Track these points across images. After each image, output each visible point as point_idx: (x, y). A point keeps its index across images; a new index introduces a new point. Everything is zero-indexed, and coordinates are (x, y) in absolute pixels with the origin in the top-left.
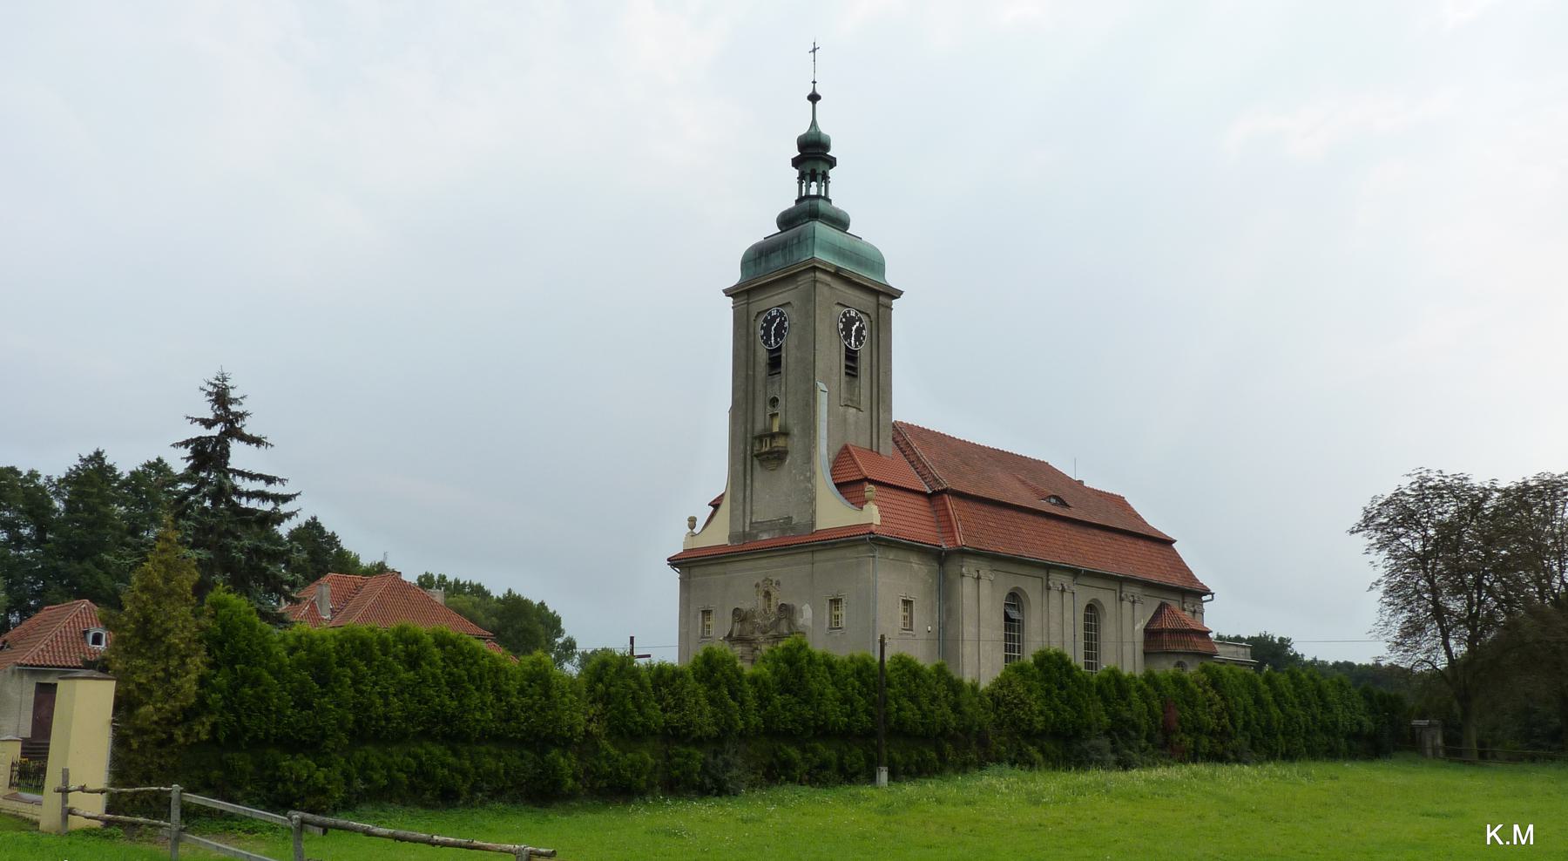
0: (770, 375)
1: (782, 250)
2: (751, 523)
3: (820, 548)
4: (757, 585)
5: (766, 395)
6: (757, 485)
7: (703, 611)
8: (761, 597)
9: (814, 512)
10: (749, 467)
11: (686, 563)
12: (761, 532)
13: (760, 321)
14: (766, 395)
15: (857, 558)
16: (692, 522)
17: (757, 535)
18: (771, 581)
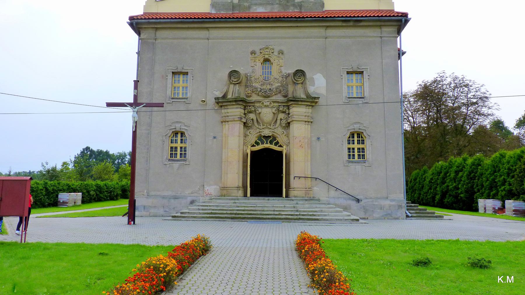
3: (340, 24)
4: (253, 53)
7: (173, 73)
8: (259, 64)
11: (155, 23)
12: (256, 4)
17: (249, 7)
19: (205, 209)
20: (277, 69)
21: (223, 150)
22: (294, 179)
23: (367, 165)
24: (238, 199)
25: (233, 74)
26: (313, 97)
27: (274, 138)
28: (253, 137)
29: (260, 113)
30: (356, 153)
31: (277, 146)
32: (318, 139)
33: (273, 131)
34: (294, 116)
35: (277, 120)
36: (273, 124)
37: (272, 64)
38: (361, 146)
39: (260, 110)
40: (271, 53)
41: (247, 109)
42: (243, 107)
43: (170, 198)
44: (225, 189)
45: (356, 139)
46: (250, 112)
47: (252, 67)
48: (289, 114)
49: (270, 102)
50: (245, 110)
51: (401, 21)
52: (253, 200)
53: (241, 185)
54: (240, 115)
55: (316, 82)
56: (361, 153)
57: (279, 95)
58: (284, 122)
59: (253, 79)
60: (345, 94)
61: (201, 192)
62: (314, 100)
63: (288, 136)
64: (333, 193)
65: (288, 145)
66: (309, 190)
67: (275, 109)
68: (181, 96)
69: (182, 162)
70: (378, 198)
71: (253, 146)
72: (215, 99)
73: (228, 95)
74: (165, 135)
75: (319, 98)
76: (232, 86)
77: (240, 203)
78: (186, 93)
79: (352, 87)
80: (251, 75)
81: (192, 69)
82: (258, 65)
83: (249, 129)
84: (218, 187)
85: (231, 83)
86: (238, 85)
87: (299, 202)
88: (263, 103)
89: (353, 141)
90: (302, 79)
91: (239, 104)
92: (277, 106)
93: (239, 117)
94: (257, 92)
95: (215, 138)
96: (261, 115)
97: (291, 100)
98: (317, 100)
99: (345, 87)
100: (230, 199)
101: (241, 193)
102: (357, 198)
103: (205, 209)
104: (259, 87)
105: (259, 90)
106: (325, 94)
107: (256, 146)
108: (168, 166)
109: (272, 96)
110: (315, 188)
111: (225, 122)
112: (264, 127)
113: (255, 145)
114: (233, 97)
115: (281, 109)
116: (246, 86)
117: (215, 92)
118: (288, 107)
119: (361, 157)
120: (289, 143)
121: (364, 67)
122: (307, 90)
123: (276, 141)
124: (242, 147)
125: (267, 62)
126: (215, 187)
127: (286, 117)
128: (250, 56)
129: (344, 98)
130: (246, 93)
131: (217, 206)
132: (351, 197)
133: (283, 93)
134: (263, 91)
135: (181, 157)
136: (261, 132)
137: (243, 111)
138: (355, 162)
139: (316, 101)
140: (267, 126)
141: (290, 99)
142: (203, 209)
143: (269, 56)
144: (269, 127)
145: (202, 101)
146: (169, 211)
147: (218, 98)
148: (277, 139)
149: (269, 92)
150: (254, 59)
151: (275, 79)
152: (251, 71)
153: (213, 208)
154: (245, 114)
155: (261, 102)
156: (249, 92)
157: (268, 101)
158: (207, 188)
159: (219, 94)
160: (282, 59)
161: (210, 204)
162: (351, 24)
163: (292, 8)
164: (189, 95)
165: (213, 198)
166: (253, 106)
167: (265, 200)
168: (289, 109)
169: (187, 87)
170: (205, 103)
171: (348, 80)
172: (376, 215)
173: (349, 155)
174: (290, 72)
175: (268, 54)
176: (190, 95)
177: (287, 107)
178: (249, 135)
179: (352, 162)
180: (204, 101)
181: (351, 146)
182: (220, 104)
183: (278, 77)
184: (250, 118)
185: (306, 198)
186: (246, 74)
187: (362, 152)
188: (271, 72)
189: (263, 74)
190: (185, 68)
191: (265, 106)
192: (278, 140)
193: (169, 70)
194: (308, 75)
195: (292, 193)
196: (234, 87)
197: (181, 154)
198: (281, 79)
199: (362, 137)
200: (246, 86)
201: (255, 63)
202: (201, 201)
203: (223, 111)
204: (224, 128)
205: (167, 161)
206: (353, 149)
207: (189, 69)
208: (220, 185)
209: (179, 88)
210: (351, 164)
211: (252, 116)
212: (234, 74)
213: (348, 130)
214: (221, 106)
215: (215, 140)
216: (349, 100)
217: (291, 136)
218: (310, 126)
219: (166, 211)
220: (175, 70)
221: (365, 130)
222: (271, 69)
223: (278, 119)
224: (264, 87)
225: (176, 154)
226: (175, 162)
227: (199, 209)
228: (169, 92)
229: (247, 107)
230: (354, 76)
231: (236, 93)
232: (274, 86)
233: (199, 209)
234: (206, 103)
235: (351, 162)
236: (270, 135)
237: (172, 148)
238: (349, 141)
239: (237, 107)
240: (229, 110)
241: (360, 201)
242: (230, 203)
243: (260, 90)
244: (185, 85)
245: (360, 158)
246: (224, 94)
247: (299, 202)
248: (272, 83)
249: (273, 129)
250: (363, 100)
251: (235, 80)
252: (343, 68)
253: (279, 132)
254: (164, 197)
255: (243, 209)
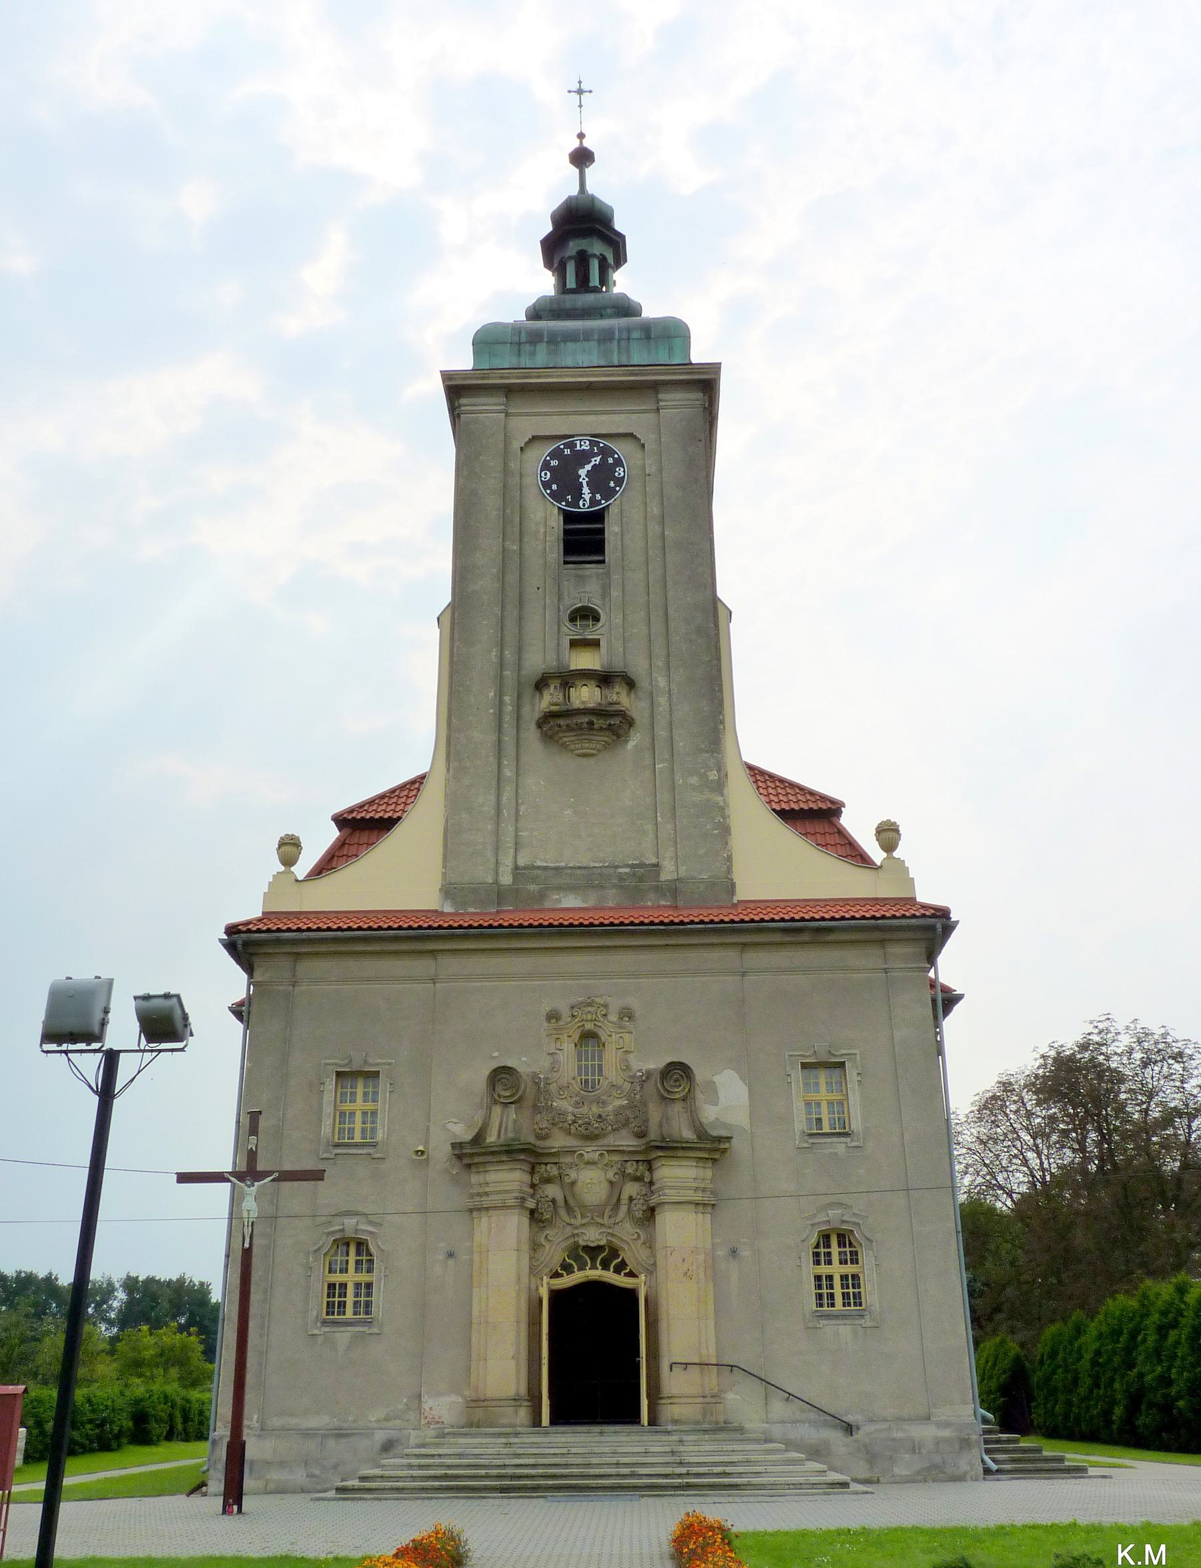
0: (566, 563)
1: (599, 341)
2: (516, 868)
3: (777, 937)
4: (553, 1016)
5: (560, 597)
6: (531, 783)
7: (339, 1074)
8: (568, 1046)
9: (729, 859)
10: (508, 739)
11: (294, 942)
12: (559, 888)
13: (543, 452)
14: (560, 597)
15: (886, 971)
16: (289, 848)
17: (542, 896)
18: (606, 1006)
19: (428, 1466)
20: (618, 1059)
21: (475, 1290)
22: (671, 1371)
23: (869, 1324)
24: (517, 1434)
25: (501, 1076)
26: (714, 1137)
27: (614, 1252)
28: (554, 1253)
29: (573, 1183)
30: (838, 1291)
31: (622, 1274)
32: (734, 1252)
33: (610, 1231)
34: (666, 1191)
35: (619, 1200)
36: (611, 1213)
37: (604, 1045)
38: (850, 1269)
39: (573, 1175)
40: (600, 1017)
41: (538, 1172)
42: (527, 1167)
43: (325, 1436)
44: (481, 1404)
45: (835, 1249)
46: (548, 1181)
47: (549, 1054)
48: (651, 1183)
49: (600, 1152)
50: (532, 1172)
51: (932, 928)
52: (559, 1435)
53: (523, 1390)
54: (521, 1191)
55: (721, 1095)
56: (851, 1290)
57: (624, 1132)
58: (639, 1209)
59: (553, 1088)
60: (800, 1123)
61: (412, 1416)
62: (716, 1145)
63: (650, 1244)
64: (779, 1408)
65: (652, 1270)
66: (714, 1400)
67: (615, 1169)
68: (358, 1139)
69: (361, 1329)
70: (900, 1419)
71: (556, 1275)
72: (454, 1145)
73: (489, 1133)
74: (316, 1251)
75: (732, 1138)
76: (497, 1109)
77: (523, 1445)
78: (373, 1130)
79: (818, 1104)
80: (548, 1078)
81: (390, 1064)
82: (566, 1049)
83: (544, 1227)
84: (461, 1400)
85: (496, 1102)
86: (513, 1105)
87: (685, 1438)
88: (582, 1155)
89: (829, 1254)
90: (682, 1087)
91: (519, 1160)
92: (620, 1163)
93: (518, 1195)
94: (566, 1125)
95: (451, 1255)
96: (577, 1188)
97: (658, 1148)
98: (727, 1145)
99: (799, 1106)
100: (493, 1435)
101: (523, 1414)
102: (846, 1421)
103: (428, 1466)
104: (570, 1109)
105: (570, 1118)
106: (748, 1127)
107: (565, 1275)
108: (320, 1340)
109: (605, 1136)
110: (730, 1396)
111: (479, 1210)
112: (585, 1221)
113: (560, 1272)
114: (502, 1141)
115: (630, 1170)
116: (536, 1109)
117: (451, 1126)
118: (649, 1164)
119: (852, 1301)
120: (655, 1264)
121: (846, 1052)
122: (698, 1118)
123: (619, 1260)
124: (525, 1281)
125: (591, 1041)
126: (453, 1399)
127: (644, 1192)
128: (546, 1025)
129: (797, 1138)
130: (536, 1127)
131: (461, 1456)
132: (828, 1418)
133: (633, 1125)
134: (580, 1122)
135: (355, 1313)
136: (577, 1234)
137: (526, 1178)
138: (837, 1317)
139: (722, 1146)
140: (593, 1218)
141: (653, 1144)
142: (421, 1467)
143: (594, 1025)
144: (600, 1220)
145: (418, 1151)
146: (323, 1476)
147: (460, 1143)
148: (622, 1255)
149: (597, 1125)
150: (555, 1032)
151: (613, 1086)
152: (547, 1065)
153: (449, 1461)
154: (533, 1186)
155: (575, 1152)
156: (544, 1126)
157: (595, 1148)
158: (428, 1403)
159: (464, 1133)
160: (631, 1033)
161: (441, 1451)
162: (806, 937)
163: (652, 895)
164: (380, 1135)
165: (446, 1431)
166: (556, 1163)
167: (592, 1435)
168: (650, 1169)
169: (374, 1113)
170: (425, 1157)
171: (806, 1085)
172: (900, 1470)
173: (820, 1297)
174: (652, 1066)
175: (591, 1021)
176: (384, 1133)
177: (645, 1164)
178: (543, 1243)
179: (828, 1317)
180: (423, 1152)
181: (823, 1270)
182: (466, 1161)
183: (620, 1082)
184: (547, 1197)
185: (706, 1426)
186: (535, 1076)
187: (854, 1288)
188: (600, 1066)
189: (580, 1074)
190: (371, 1061)
191: (588, 1163)
192: (623, 1258)
193: (328, 1067)
194: (700, 1074)
195: (668, 1411)
196: (503, 1112)
197: (356, 1304)
198: (627, 1086)
199: (851, 1245)
200: (536, 1109)
201: (559, 1044)
202: (413, 1441)
203: (475, 1179)
204: (475, 1226)
205: (319, 1324)
206: (830, 1278)
207: (384, 1064)
208: (467, 1393)
209: (352, 1114)
210: (825, 1322)
211: (552, 1191)
212: (503, 1076)
213: (812, 1225)
214: (469, 1166)
215: (451, 1262)
216: (811, 1141)
217: (658, 1246)
218: (710, 1215)
219: (312, 1476)
220: (343, 1066)
221: (858, 1224)
222: (600, 1058)
223: (622, 1197)
224: (584, 1110)
225: (342, 1305)
226: (342, 1329)
227: (410, 1466)
228: (326, 1129)
229: (537, 1168)
230: (822, 1076)
231: (509, 1129)
232: (610, 1108)
233: (410, 1466)
234: (428, 1158)
235: (823, 1318)
236: (602, 1243)
237: (331, 1286)
238: (817, 1255)
239: (512, 1166)
240: (491, 1177)
241: (854, 1429)
242: (497, 1446)
243: (573, 1118)
244: (370, 1106)
245: (849, 1305)
246: (478, 1133)
247: (685, 1438)
248: (604, 1098)
249: (610, 1228)
250: (848, 1140)
251: (508, 1094)
252: (792, 1053)
253: (626, 1233)
254: (307, 1434)
255: (531, 1461)
